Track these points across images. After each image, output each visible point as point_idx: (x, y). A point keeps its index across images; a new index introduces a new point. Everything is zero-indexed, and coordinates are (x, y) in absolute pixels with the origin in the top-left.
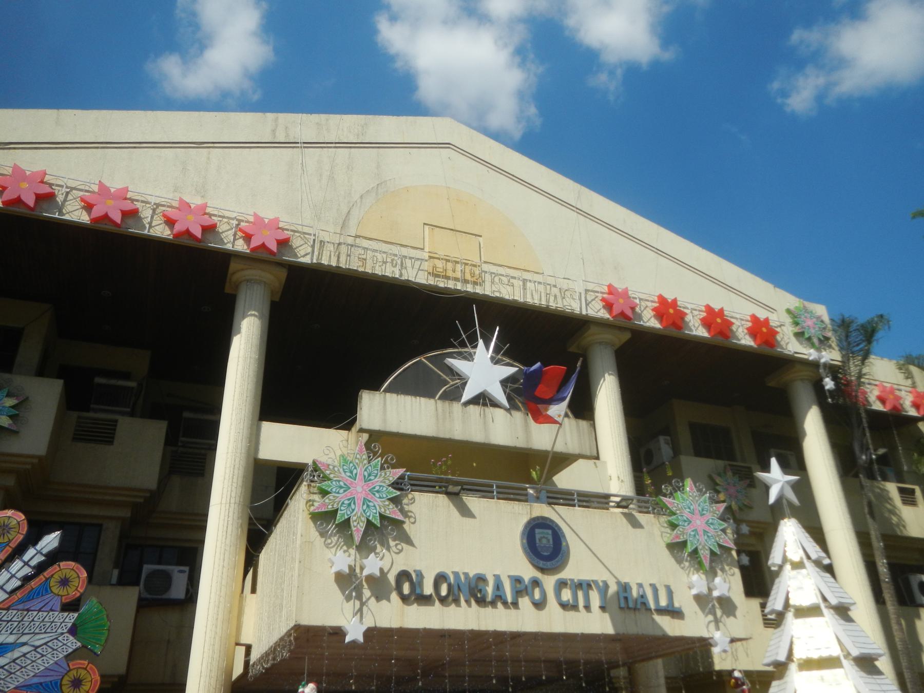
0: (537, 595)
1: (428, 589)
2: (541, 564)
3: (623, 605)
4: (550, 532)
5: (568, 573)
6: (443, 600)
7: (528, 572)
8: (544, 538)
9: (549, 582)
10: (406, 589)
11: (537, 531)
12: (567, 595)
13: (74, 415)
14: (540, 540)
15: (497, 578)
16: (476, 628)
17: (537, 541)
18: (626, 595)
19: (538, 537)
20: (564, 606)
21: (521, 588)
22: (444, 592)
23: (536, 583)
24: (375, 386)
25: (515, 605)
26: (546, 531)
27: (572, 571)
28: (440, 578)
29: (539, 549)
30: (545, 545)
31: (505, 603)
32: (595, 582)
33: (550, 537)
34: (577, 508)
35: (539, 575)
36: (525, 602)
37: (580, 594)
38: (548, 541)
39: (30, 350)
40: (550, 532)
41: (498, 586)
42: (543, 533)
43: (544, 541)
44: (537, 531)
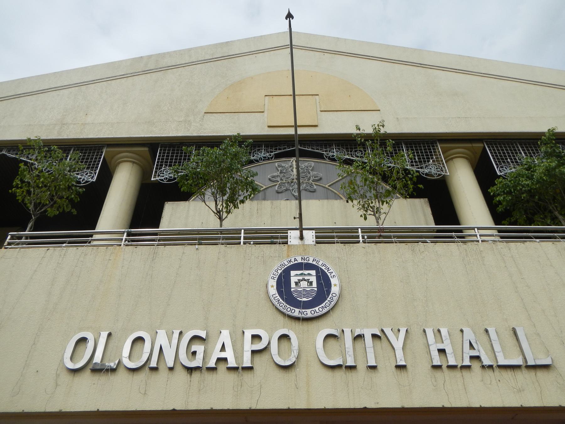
2: (296, 312)
3: (437, 362)
4: (313, 272)
5: (344, 322)
8: (304, 283)
11: (293, 273)
14: (297, 284)
16: (179, 406)
17: (293, 285)
18: (441, 347)
19: (293, 280)
26: (306, 272)
29: (295, 295)
33: (313, 279)
34: (361, 245)
38: (311, 283)
40: (313, 272)
42: (302, 274)
43: (304, 284)
44: (293, 273)
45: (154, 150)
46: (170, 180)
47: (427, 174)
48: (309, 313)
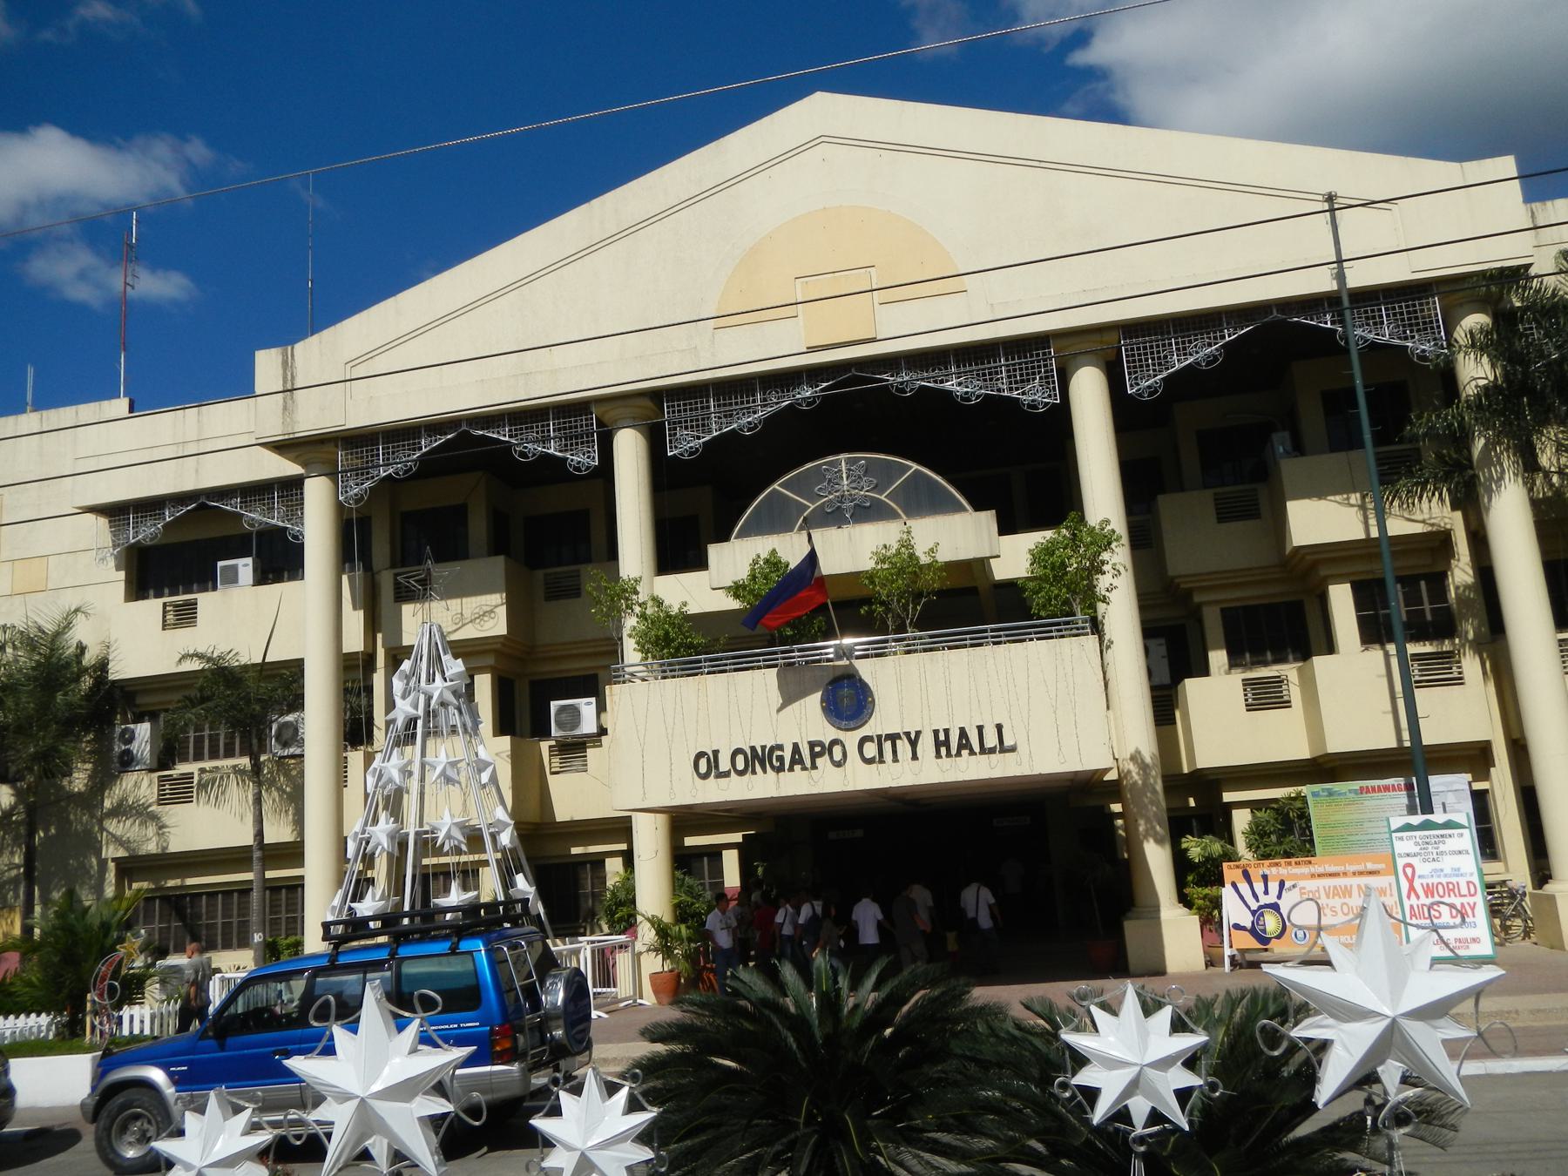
0: (837, 751)
1: (724, 765)
6: (741, 773)
7: (827, 732)
9: (851, 739)
10: (703, 768)
12: (870, 750)
13: (540, 574)
15: (796, 748)
21: (819, 750)
22: (740, 765)
23: (835, 742)
24: (723, 537)
25: (814, 767)
30: (848, 700)
31: (804, 769)
32: (908, 734)
35: (841, 735)
36: (823, 762)
37: (887, 746)
39: (478, 527)
41: (796, 748)
45: (657, 407)
46: (691, 454)
47: (1029, 406)
48: (852, 725)
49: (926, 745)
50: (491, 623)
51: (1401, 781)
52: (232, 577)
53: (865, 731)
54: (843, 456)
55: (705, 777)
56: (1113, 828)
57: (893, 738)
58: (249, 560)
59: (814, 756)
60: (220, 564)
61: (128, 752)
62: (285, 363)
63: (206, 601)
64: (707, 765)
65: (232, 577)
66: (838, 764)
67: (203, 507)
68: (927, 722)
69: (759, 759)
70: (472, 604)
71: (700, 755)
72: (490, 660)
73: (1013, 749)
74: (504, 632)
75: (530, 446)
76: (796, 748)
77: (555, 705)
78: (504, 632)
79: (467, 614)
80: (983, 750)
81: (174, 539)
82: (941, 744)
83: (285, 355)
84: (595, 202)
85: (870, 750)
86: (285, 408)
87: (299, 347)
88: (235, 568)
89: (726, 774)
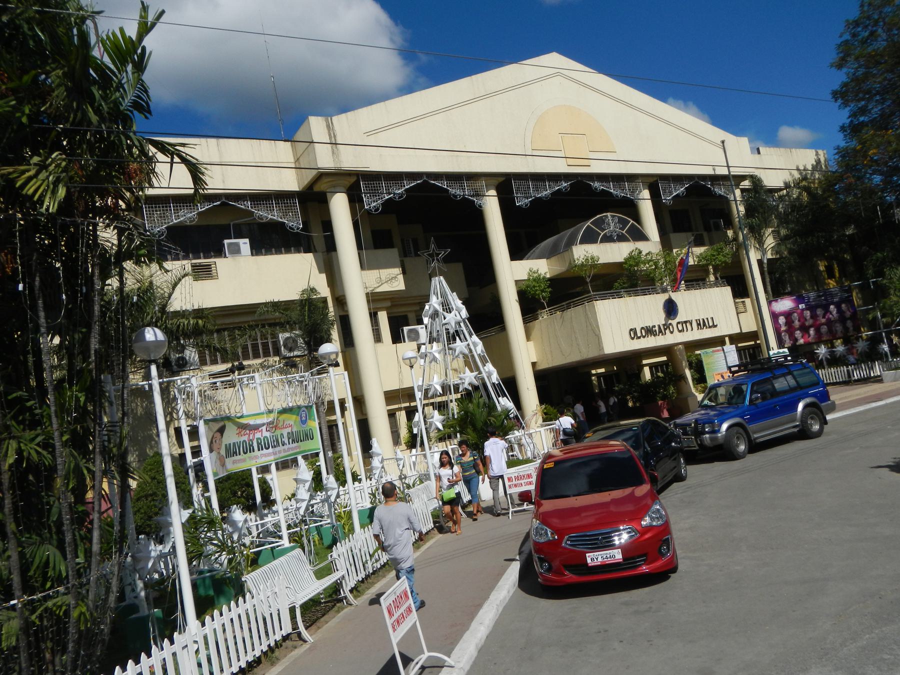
1: (639, 335)
6: (644, 337)
9: (674, 322)
15: (659, 326)
20: (680, 331)
27: (681, 317)
28: (642, 328)
36: (667, 331)
49: (695, 325)
50: (396, 283)
51: (720, 348)
52: (236, 250)
53: (677, 320)
54: (609, 214)
55: (633, 339)
56: (591, 381)
57: (686, 322)
58: (247, 240)
59: (665, 329)
60: (226, 242)
61: (183, 358)
62: (328, 127)
63: (221, 265)
64: (633, 334)
65: (236, 250)
66: (672, 333)
67: (223, 204)
68: (694, 316)
69: (649, 331)
70: (386, 273)
71: (631, 330)
72: (388, 304)
73: (716, 326)
74: (404, 288)
75: (455, 191)
76: (659, 326)
77: (406, 329)
78: (404, 288)
79: (383, 278)
80: (710, 327)
81: (204, 223)
82: (699, 324)
83: (327, 121)
84: (473, 77)
85: (680, 328)
86: (333, 153)
87: (335, 119)
88: (238, 245)
89: (639, 338)
